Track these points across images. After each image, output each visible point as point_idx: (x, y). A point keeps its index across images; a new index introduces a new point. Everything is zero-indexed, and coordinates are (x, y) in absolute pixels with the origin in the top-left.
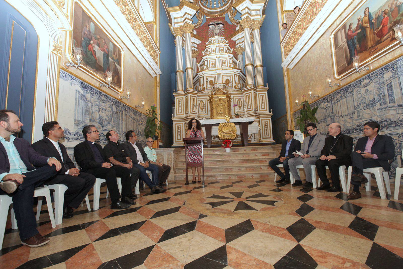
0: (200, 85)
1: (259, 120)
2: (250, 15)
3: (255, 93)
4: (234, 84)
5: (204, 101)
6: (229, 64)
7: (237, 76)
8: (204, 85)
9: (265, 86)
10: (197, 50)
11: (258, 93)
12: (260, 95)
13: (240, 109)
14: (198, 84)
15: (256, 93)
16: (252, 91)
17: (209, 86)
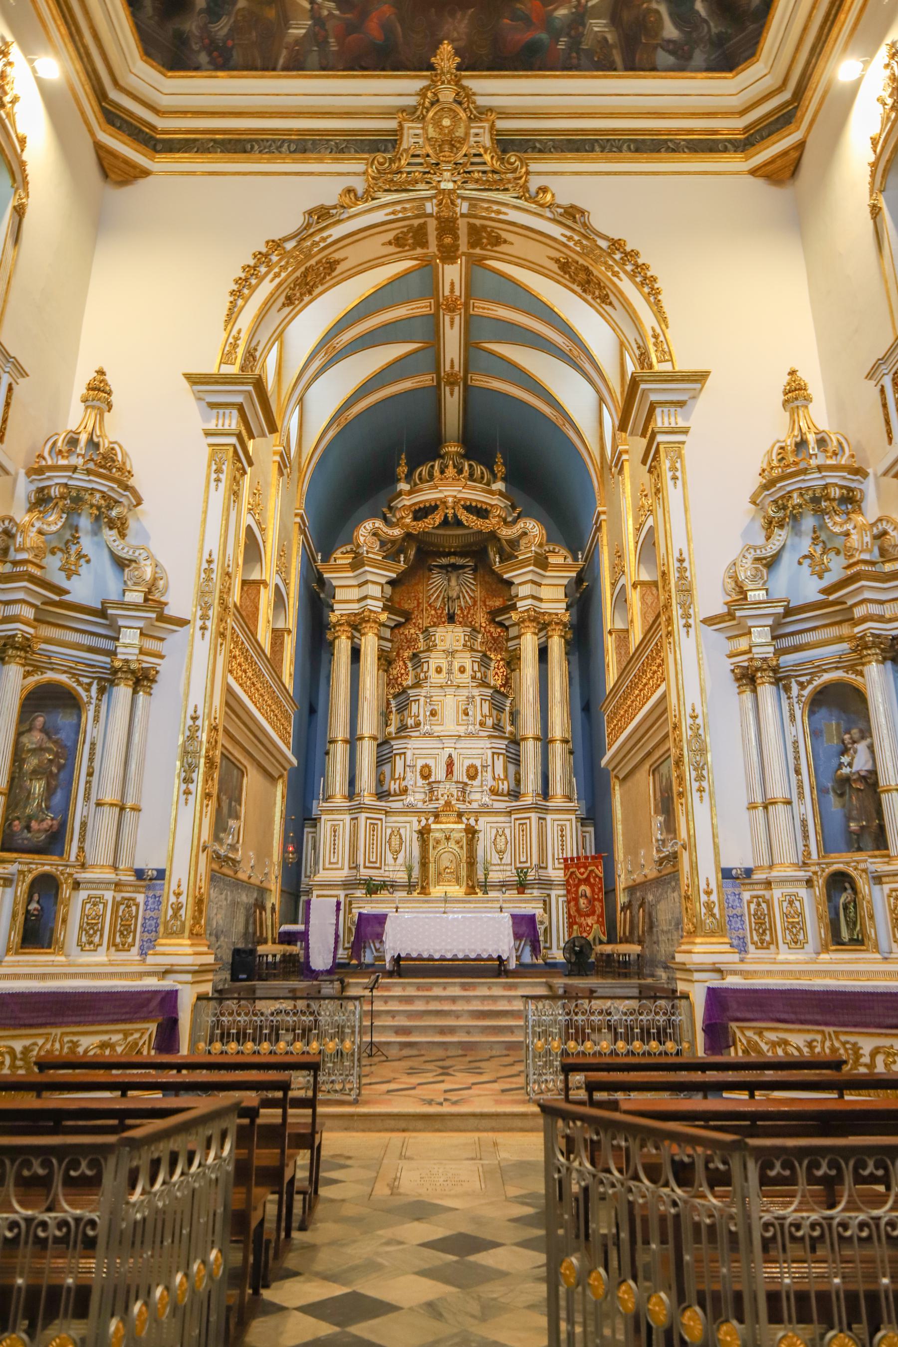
0: (393, 778)
1: (549, 895)
2: (540, 600)
3: (540, 818)
4: (491, 783)
5: (402, 831)
6: (479, 718)
7: (501, 757)
8: (404, 779)
9: (570, 799)
10: (389, 645)
11: (549, 817)
12: (556, 823)
13: (501, 859)
14: (387, 768)
15: (544, 819)
16: (534, 816)
17: (420, 782)
